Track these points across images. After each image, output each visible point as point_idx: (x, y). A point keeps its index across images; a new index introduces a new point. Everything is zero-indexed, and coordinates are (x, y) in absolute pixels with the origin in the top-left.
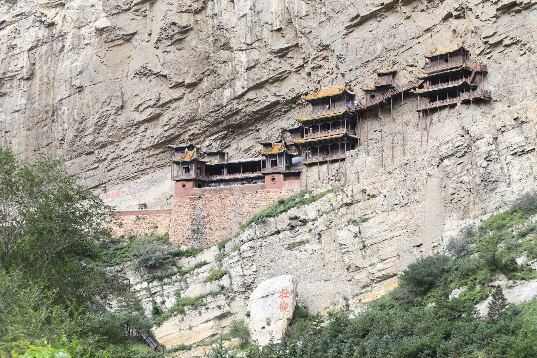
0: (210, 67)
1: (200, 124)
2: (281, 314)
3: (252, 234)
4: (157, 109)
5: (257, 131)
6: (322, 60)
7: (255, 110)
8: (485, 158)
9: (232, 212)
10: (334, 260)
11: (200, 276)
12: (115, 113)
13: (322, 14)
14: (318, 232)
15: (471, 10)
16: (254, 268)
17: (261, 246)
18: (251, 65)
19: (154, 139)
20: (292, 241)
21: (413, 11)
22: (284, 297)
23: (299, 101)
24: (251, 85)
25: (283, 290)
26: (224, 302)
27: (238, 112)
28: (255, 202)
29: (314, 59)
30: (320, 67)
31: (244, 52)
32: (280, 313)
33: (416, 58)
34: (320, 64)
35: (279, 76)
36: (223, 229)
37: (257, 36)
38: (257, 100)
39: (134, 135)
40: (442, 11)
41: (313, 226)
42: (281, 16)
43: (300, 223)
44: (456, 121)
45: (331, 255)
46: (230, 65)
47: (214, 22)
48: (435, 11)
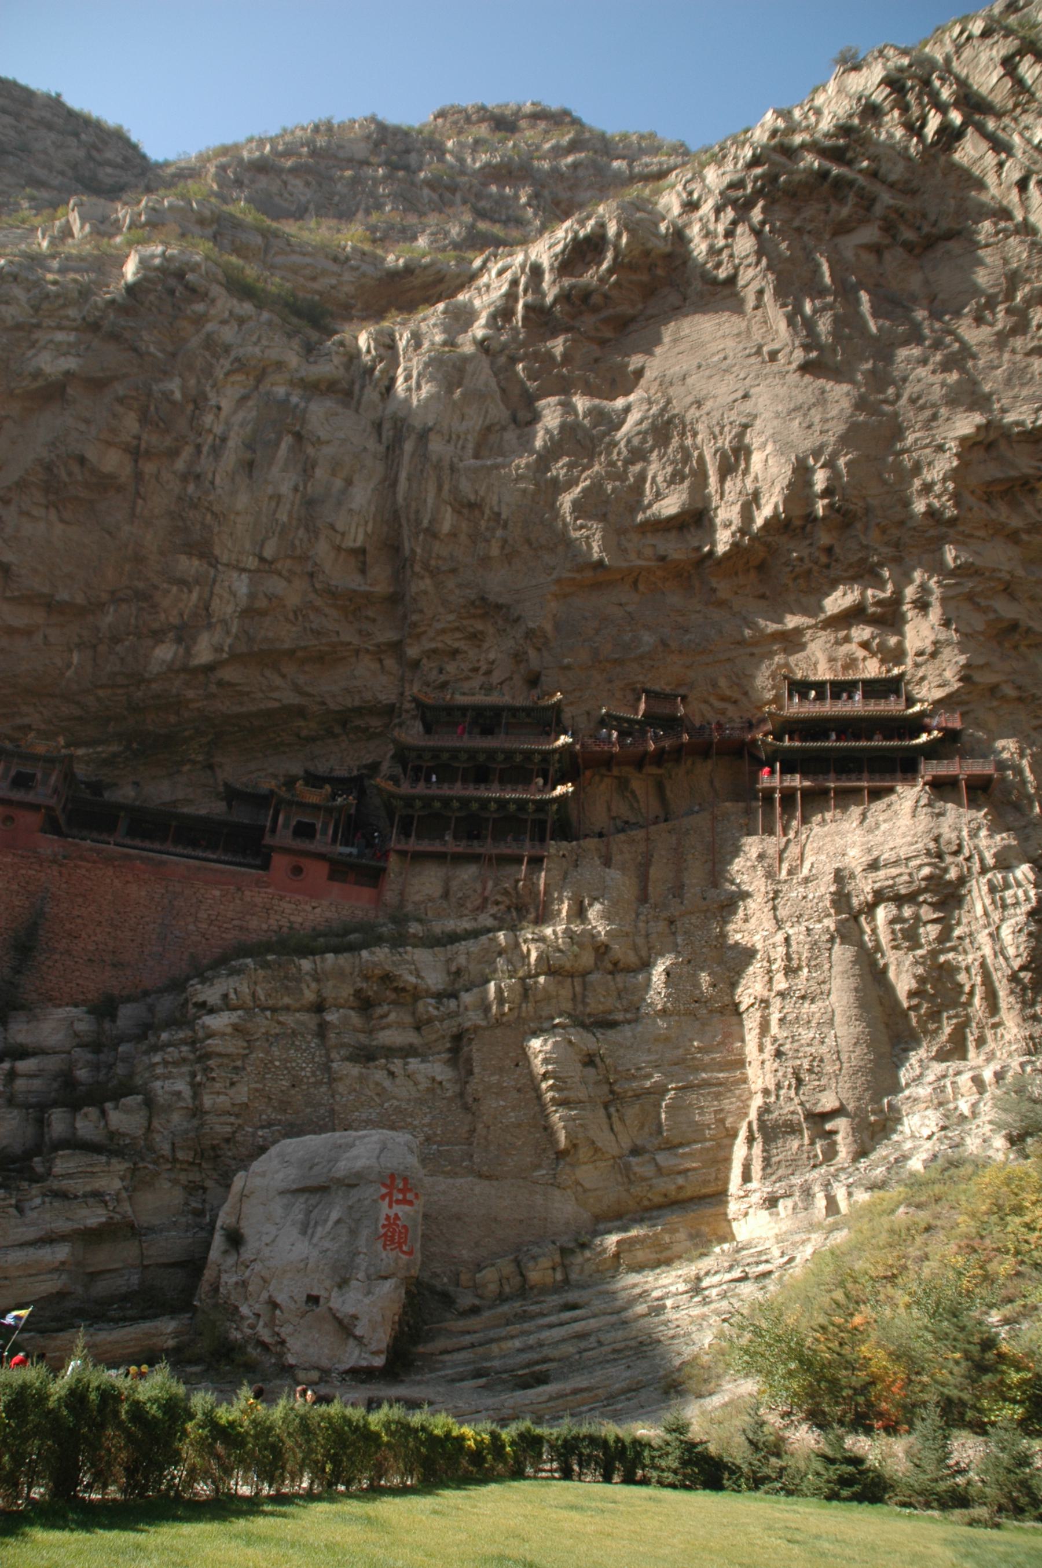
2: (387, 1257)
3: (245, 989)
5: (211, 767)
8: (1031, 914)
9: (152, 926)
10: (512, 1117)
11: (20, 1084)
13: (493, 542)
14: (455, 1030)
16: (242, 1093)
17: (267, 1033)
18: (257, 605)
20: (363, 1038)
21: (736, 593)
22: (398, 1202)
23: (360, 722)
25: (392, 1176)
26: (117, 1184)
28: (230, 914)
29: (443, 631)
30: (455, 653)
31: (244, 576)
32: (384, 1255)
34: (456, 645)
36: (114, 965)
37: (293, 546)
38: (247, 689)
40: (838, 601)
41: (436, 1013)
42: (370, 525)
43: (393, 996)
44: (904, 820)
45: (502, 1103)
46: (195, 596)
47: (185, 489)
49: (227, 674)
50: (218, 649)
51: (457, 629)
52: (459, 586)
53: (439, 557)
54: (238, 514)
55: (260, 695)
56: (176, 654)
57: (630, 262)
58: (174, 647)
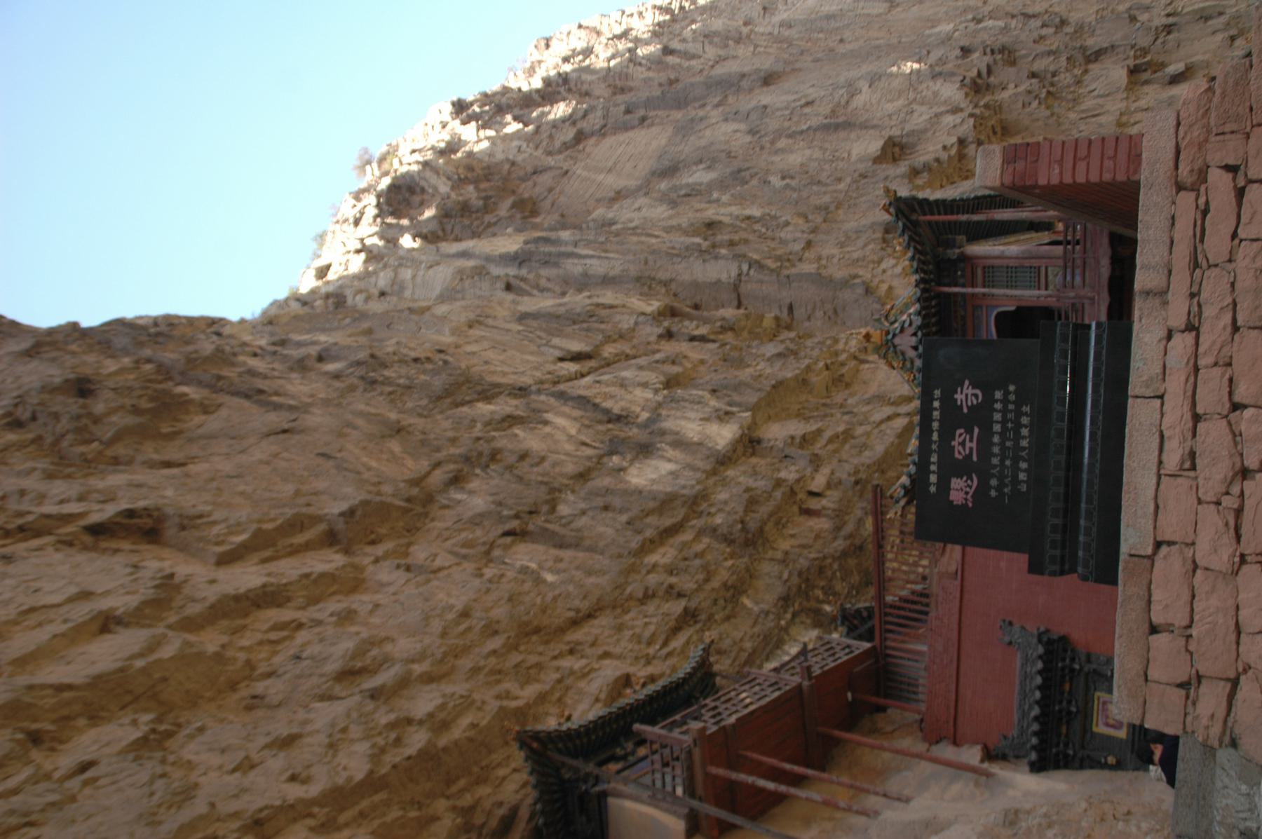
46: (560, 421)
48: (1083, 107)
53: (774, 249)
57: (466, 178)
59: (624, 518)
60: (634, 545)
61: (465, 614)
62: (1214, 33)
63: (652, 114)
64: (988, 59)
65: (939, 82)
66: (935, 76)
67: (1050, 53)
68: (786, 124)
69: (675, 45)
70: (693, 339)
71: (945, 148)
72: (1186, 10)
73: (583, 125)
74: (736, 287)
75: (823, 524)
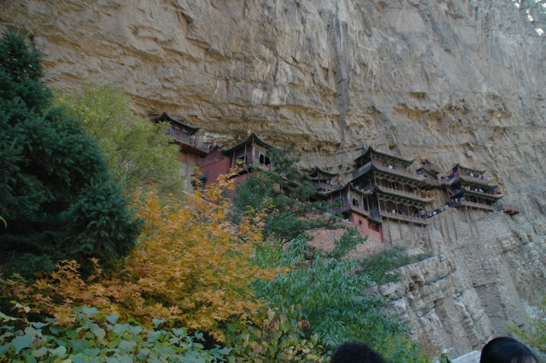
0: (245, 52)
1: (209, 109)
4: (162, 51)
6: (365, 122)
7: (283, 131)
12: (105, 7)
14: (435, 299)
15: (485, 148)
19: (143, 87)
23: (325, 147)
24: (291, 102)
27: (263, 122)
29: (359, 117)
31: (288, 65)
33: (442, 162)
34: (363, 124)
35: (318, 111)
38: (291, 122)
39: (116, 62)
46: (269, 68)
48: (452, 136)
49: (284, 112)
50: (282, 99)
51: (363, 117)
52: (364, 99)
53: (357, 84)
54: (286, 34)
55: (295, 126)
56: (263, 95)
58: (262, 92)
59: (239, 96)
60: (231, 101)
61: (194, 86)
62: (486, 159)
63: (430, 23)
64: (462, 107)
65: (449, 98)
66: (450, 96)
67: (469, 122)
68: (427, 63)
69: (479, 10)
70: (314, 80)
71: (424, 108)
72: (519, 149)
73: (421, 5)
74: (342, 80)
75: (260, 129)
